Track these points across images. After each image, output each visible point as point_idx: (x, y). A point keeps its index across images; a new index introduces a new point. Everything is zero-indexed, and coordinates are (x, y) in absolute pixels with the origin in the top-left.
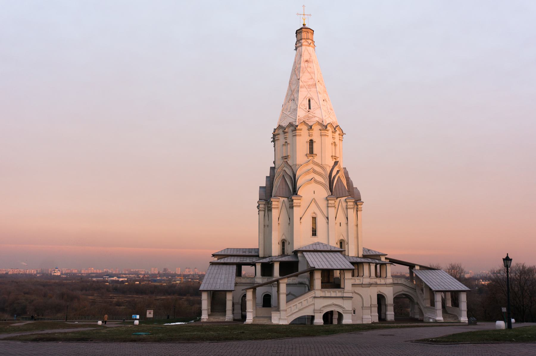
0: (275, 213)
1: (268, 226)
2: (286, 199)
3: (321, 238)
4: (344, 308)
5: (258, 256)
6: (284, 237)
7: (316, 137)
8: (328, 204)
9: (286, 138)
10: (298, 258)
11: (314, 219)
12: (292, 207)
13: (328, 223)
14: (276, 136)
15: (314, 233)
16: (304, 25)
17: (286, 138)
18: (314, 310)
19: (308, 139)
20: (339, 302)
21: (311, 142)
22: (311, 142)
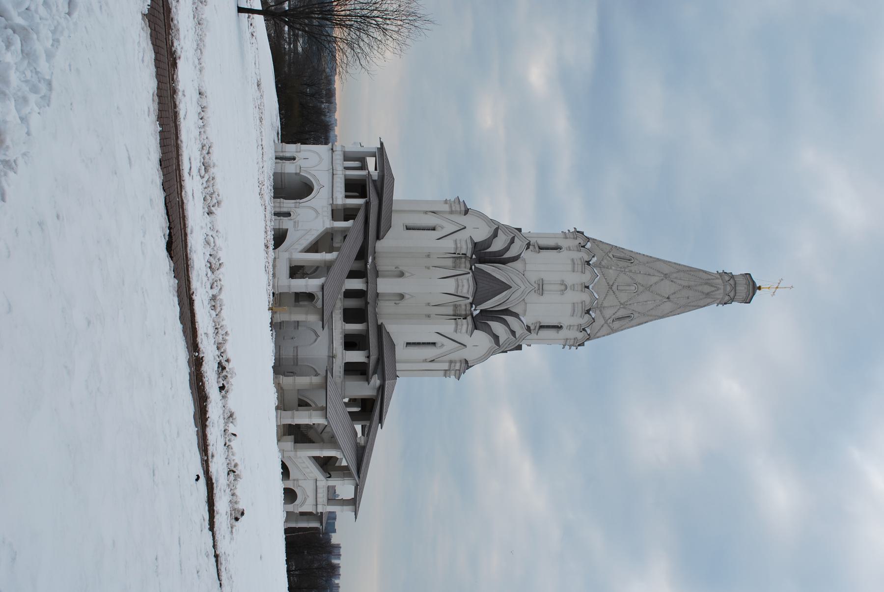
0: (450, 285)
1: (428, 256)
2: (471, 300)
3: (401, 352)
4: (301, 506)
5: (378, 237)
6: (407, 296)
7: (563, 333)
8: (455, 362)
9: (573, 287)
10: (375, 373)
11: (434, 344)
12: (456, 316)
13: (425, 361)
14: (580, 266)
15: (408, 344)
16: (759, 288)
17: (573, 287)
18: (297, 480)
19: (565, 322)
20: (310, 501)
21: (558, 327)
22: (558, 327)
